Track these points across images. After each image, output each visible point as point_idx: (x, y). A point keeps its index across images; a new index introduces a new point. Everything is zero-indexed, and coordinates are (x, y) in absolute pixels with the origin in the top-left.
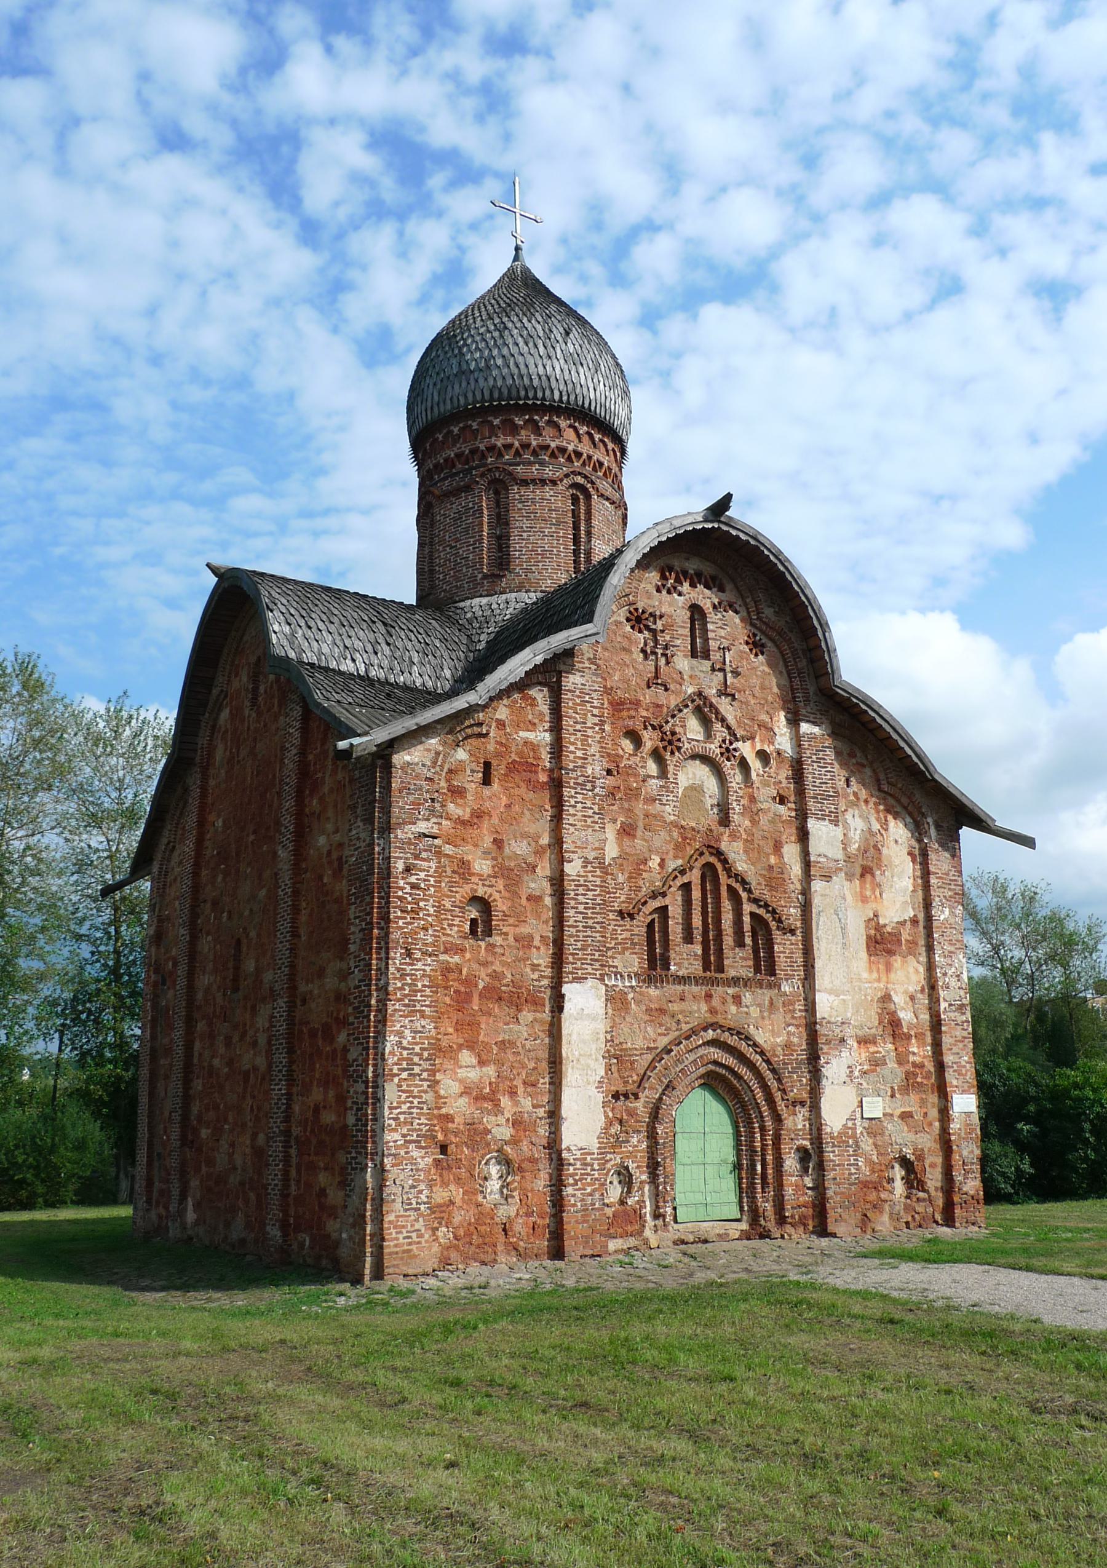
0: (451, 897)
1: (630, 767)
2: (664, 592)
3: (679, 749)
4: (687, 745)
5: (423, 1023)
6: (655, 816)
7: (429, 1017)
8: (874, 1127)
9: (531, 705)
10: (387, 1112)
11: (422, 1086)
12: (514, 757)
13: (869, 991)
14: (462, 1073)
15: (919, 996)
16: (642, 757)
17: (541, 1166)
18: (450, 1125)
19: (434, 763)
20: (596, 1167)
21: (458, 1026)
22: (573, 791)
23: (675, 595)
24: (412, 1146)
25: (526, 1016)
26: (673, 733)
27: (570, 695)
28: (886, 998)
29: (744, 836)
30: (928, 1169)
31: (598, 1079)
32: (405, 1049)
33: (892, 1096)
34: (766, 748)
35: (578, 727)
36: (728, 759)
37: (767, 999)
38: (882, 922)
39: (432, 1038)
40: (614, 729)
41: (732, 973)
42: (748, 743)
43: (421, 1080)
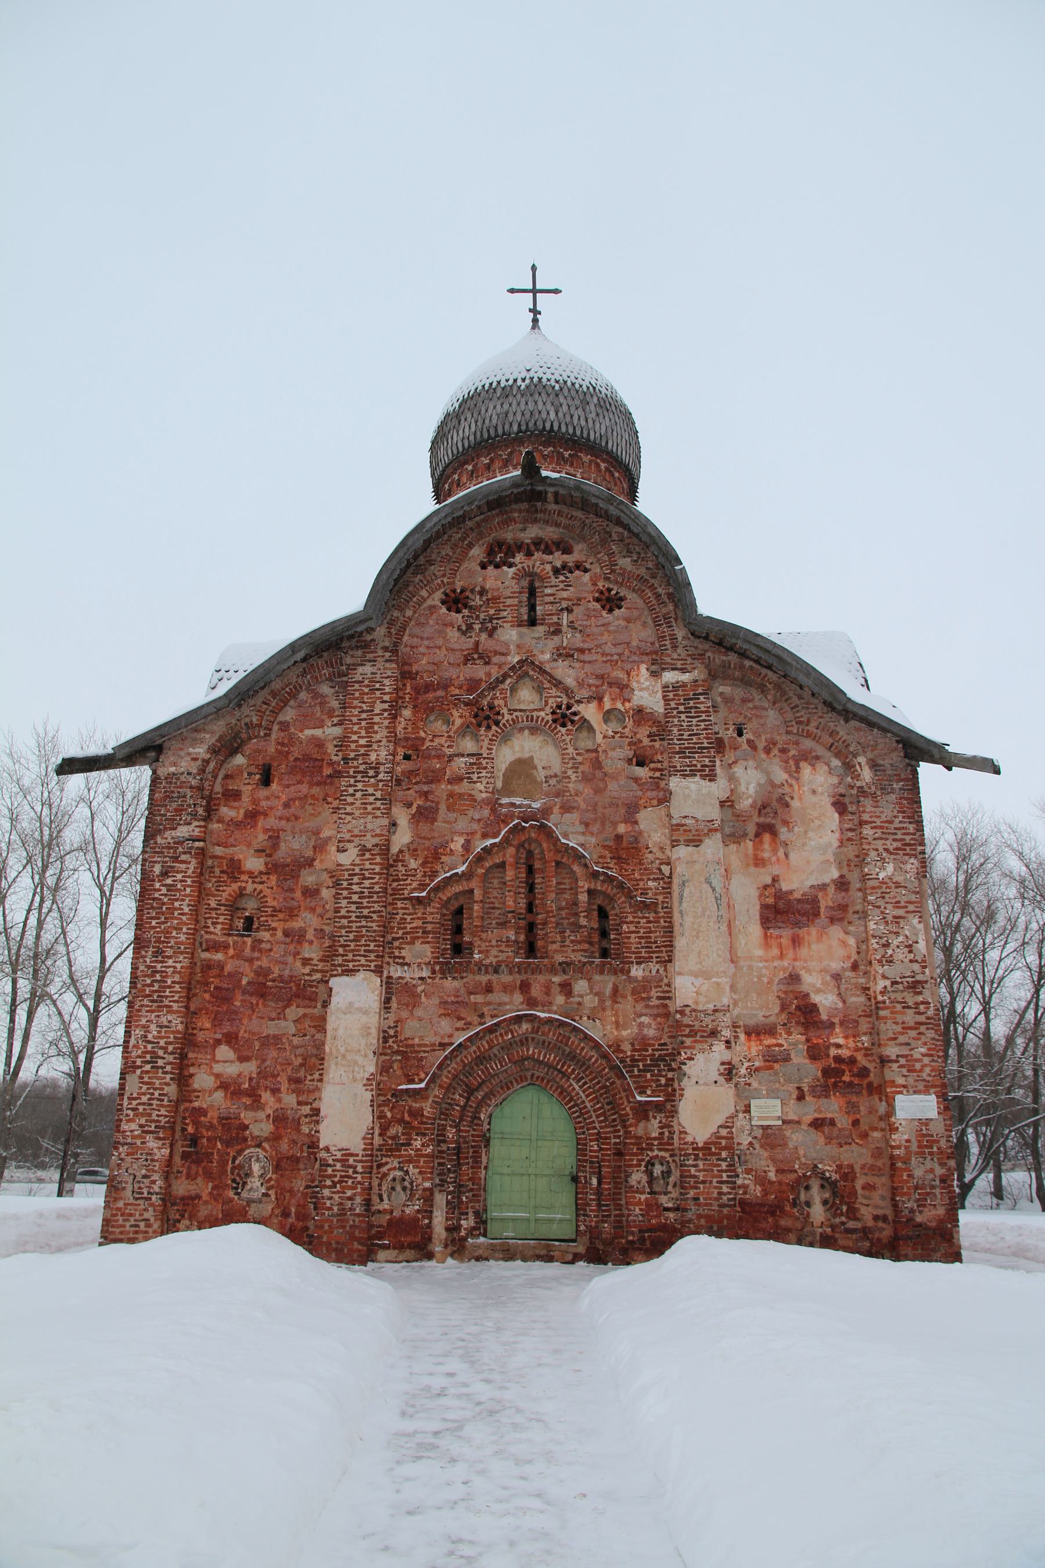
0: (218, 896)
2: (490, 568)
4: (507, 717)
5: (170, 1018)
8: (770, 1138)
10: (125, 1102)
13: (764, 971)
14: (218, 1068)
15: (848, 974)
16: (449, 737)
17: (301, 1166)
18: (202, 1118)
19: (202, 771)
20: (359, 1169)
21: (217, 1022)
22: (352, 781)
23: (505, 568)
24: (149, 1137)
25: (293, 1012)
26: (491, 707)
27: (357, 686)
28: (794, 978)
30: (860, 1191)
31: (367, 1076)
32: (150, 1042)
33: (801, 1097)
34: (619, 705)
35: (364, 715)
36: (564, 725)
37: (610, 986)
38: (785, 887)
39: (178, 1032)
40: (414, 713)
41: (559, 958)
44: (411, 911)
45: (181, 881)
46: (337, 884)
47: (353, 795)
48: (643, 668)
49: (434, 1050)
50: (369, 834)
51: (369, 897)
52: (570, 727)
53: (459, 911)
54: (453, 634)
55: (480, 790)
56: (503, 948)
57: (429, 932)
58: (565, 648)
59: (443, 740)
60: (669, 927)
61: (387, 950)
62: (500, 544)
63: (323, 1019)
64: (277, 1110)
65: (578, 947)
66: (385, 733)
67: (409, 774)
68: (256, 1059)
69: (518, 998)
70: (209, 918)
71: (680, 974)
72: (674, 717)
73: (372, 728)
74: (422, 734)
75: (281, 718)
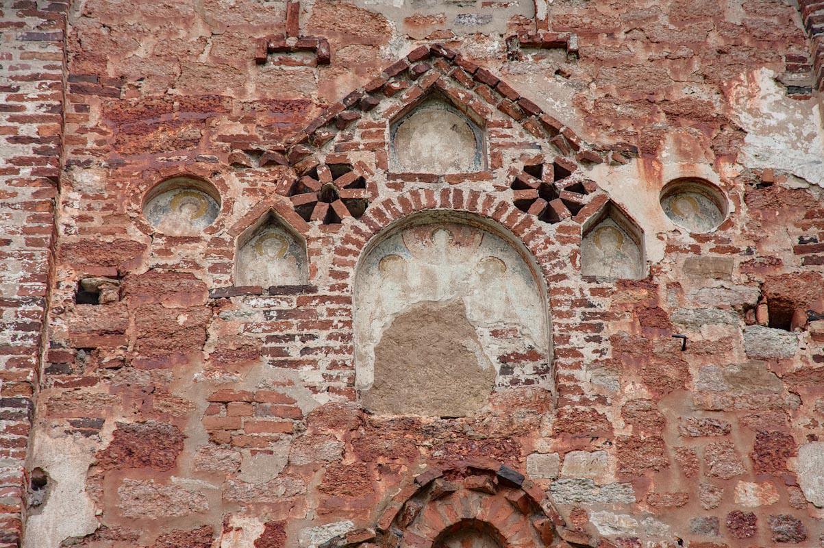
1: (172, 272)
4: (385, 192)
6: (251, 401)
16: (218, 242)
26: (339, 169)
29: (622, 430)
34: (704, 170)
36: (549, 216)
42: (631, 170)
48: (764, 77)
52: (568, 222)
58: (541, 24)
74: (137, 236)
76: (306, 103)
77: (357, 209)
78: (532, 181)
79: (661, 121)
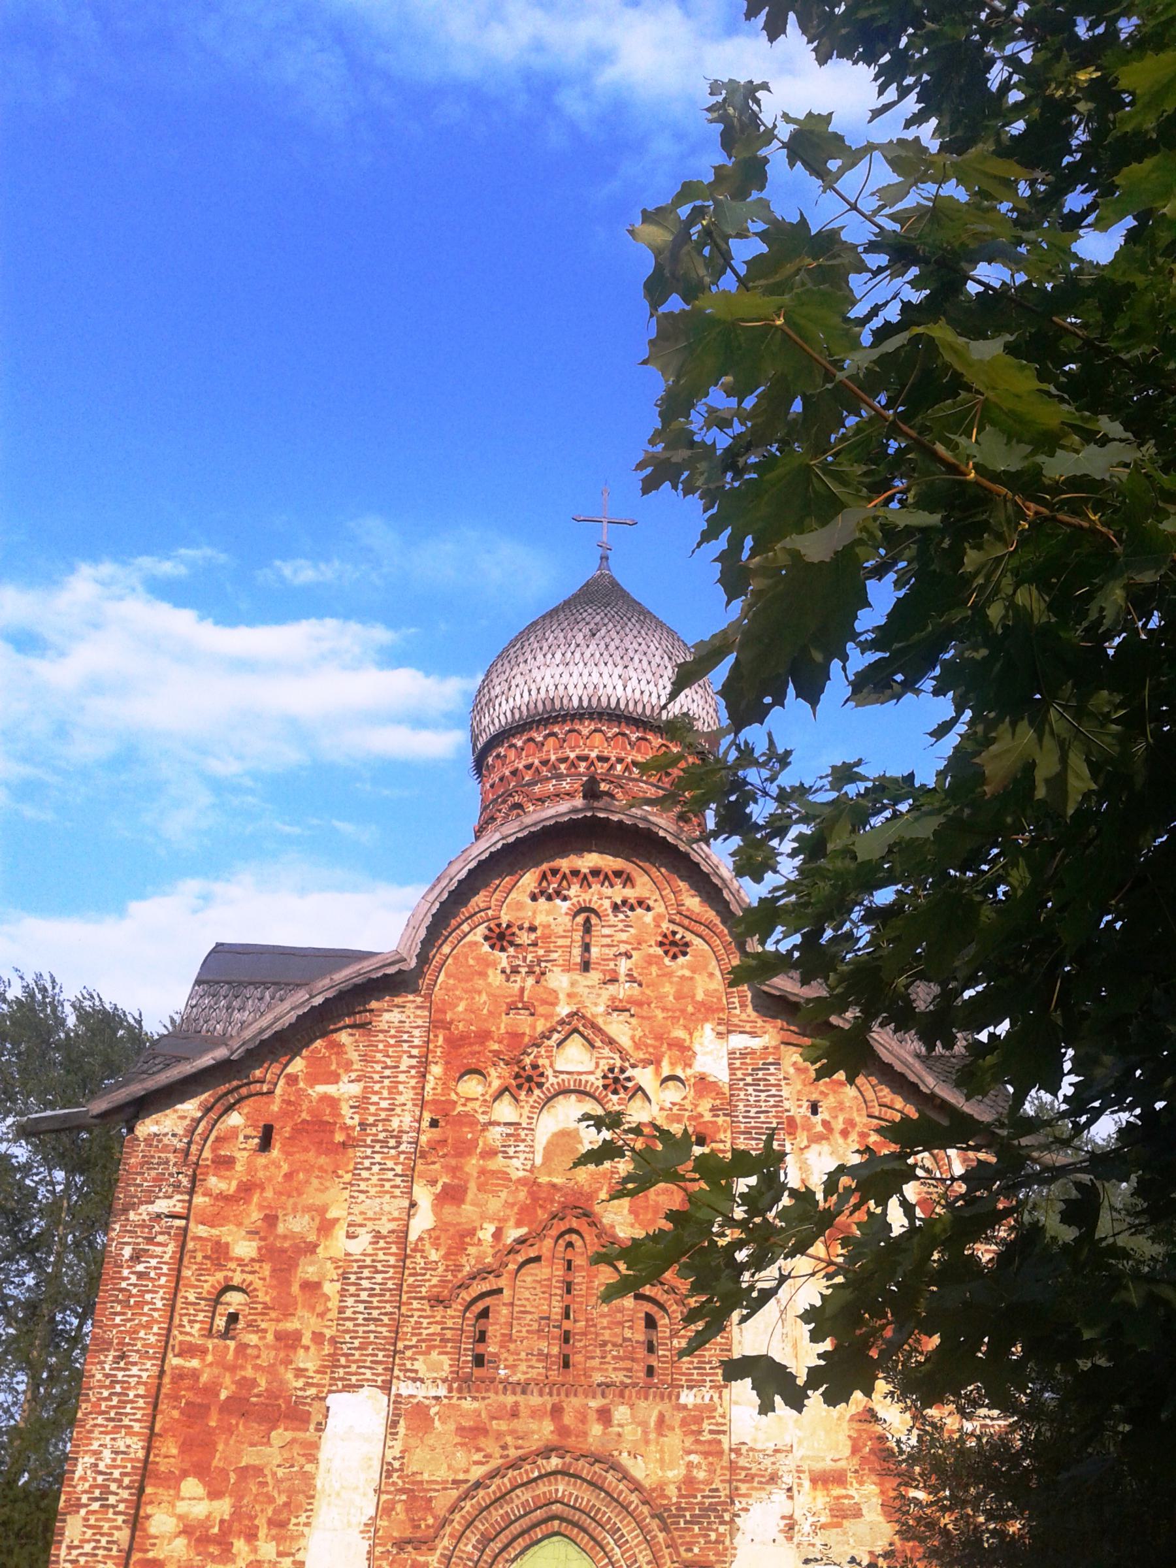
0: (197, 1287)
1: (467, 1114)
2: (542, 900)
3: (540, 1085)
4: (552, 1080)
5: (128, 1441)
6: (493, 1172)
7: (138, 1434)
9: (338, 1054)
10: (63, 1552)
11: (115, 1520)
12: (304, 1115)
14: (182, 1507)
16: (485, 1101)
19: (191, 1131)
21: (186, 1447)
22: (369, 1151)
23: (558, 901)
25: (280, 1436)
26: (535, 1066)
27: (381, 1036)
31: (365, 1520)
32: (101, 1473)
34: (679, 1072)
35: (387, 1072)
36: (615, 1092)
37: (655, 1414)
41: (598, 1378)
43: (115, 1513)
44: (429, 1313)
45: (155, 1268)
46: (344, 1277)
47: (369, 1169)
49: (445, 1489)
50: (384, 1218)
51: (381, 1295)
52: (622, 1095)
53: (485, 1314)
54: (495, 978)
55: (516, 1168)
56: (534, 1363)
57: (448, 1340)
58: (621, 1001)
59: (476, 1105)
60: (726, 1344)
61: (397, 1361)
62: (555, 872)
63: (315, 1446)
64: (251, 1562)
65: (621, 1364)
66: (410, 1094)
67: (435, 1145)
68: (231, 1496)
69: (548, 1427)
70: (186, 1314)
71: (736, 1403)
72: (740, 1089)
73: (396, 1087)
74: (454, 1097)
75: (289, 1070)
76: (524, 1034)
77: (540, 1085)
78: (610, 1075)
79: (664, 1048)
